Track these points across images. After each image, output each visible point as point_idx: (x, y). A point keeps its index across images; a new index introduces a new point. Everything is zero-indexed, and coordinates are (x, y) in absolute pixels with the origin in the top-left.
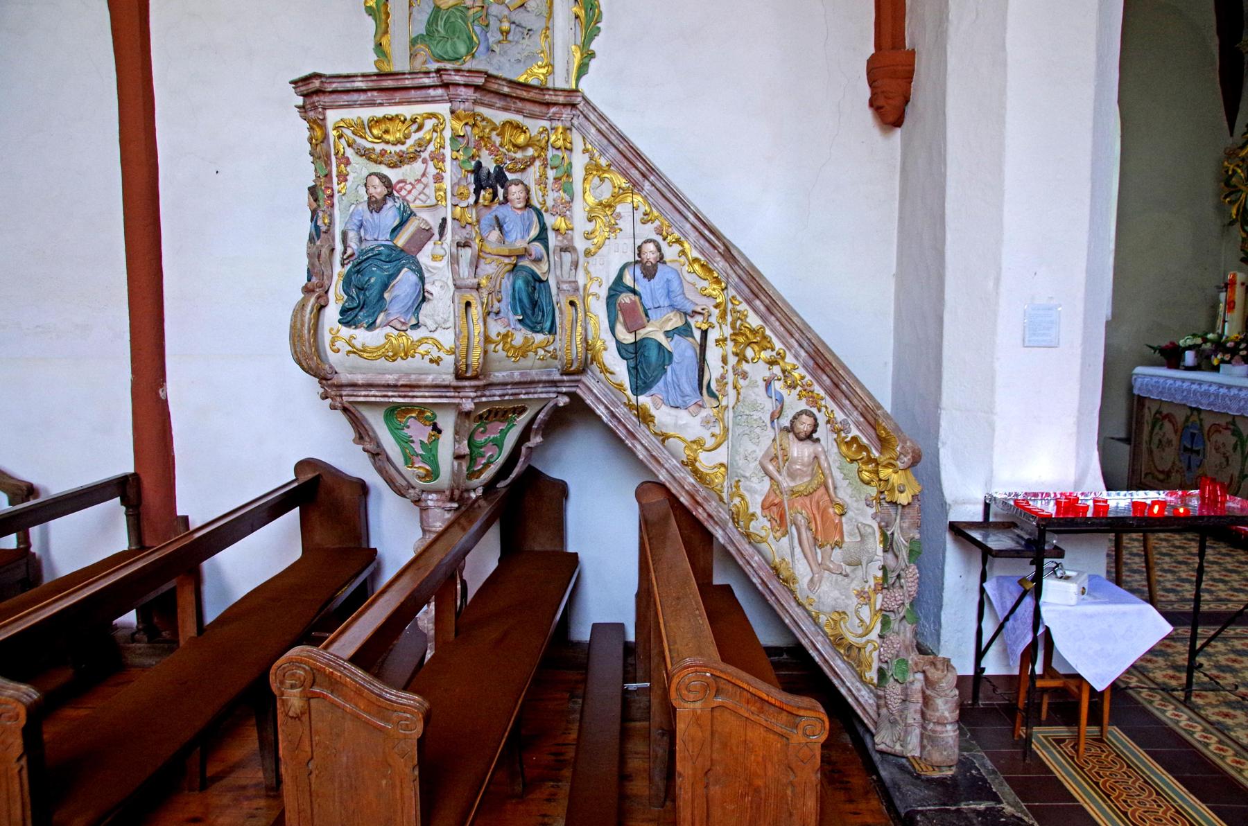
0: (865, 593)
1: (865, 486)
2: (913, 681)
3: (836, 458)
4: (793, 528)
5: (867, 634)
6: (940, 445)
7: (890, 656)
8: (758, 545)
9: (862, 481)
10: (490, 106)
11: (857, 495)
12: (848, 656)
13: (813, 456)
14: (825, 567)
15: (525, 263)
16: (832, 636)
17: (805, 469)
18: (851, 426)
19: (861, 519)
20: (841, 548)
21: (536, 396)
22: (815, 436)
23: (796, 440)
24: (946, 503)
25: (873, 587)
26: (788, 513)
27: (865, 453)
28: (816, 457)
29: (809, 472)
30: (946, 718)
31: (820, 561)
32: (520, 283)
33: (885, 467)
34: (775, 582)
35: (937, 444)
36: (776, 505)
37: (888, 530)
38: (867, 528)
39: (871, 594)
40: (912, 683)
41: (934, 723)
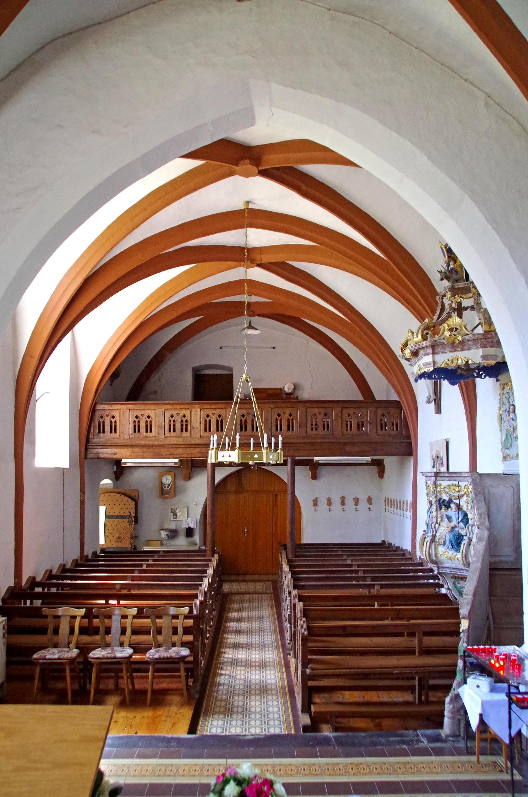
10: (444, 480)
15: (457, 529)
21: (464, 574)
32: (451, 536)
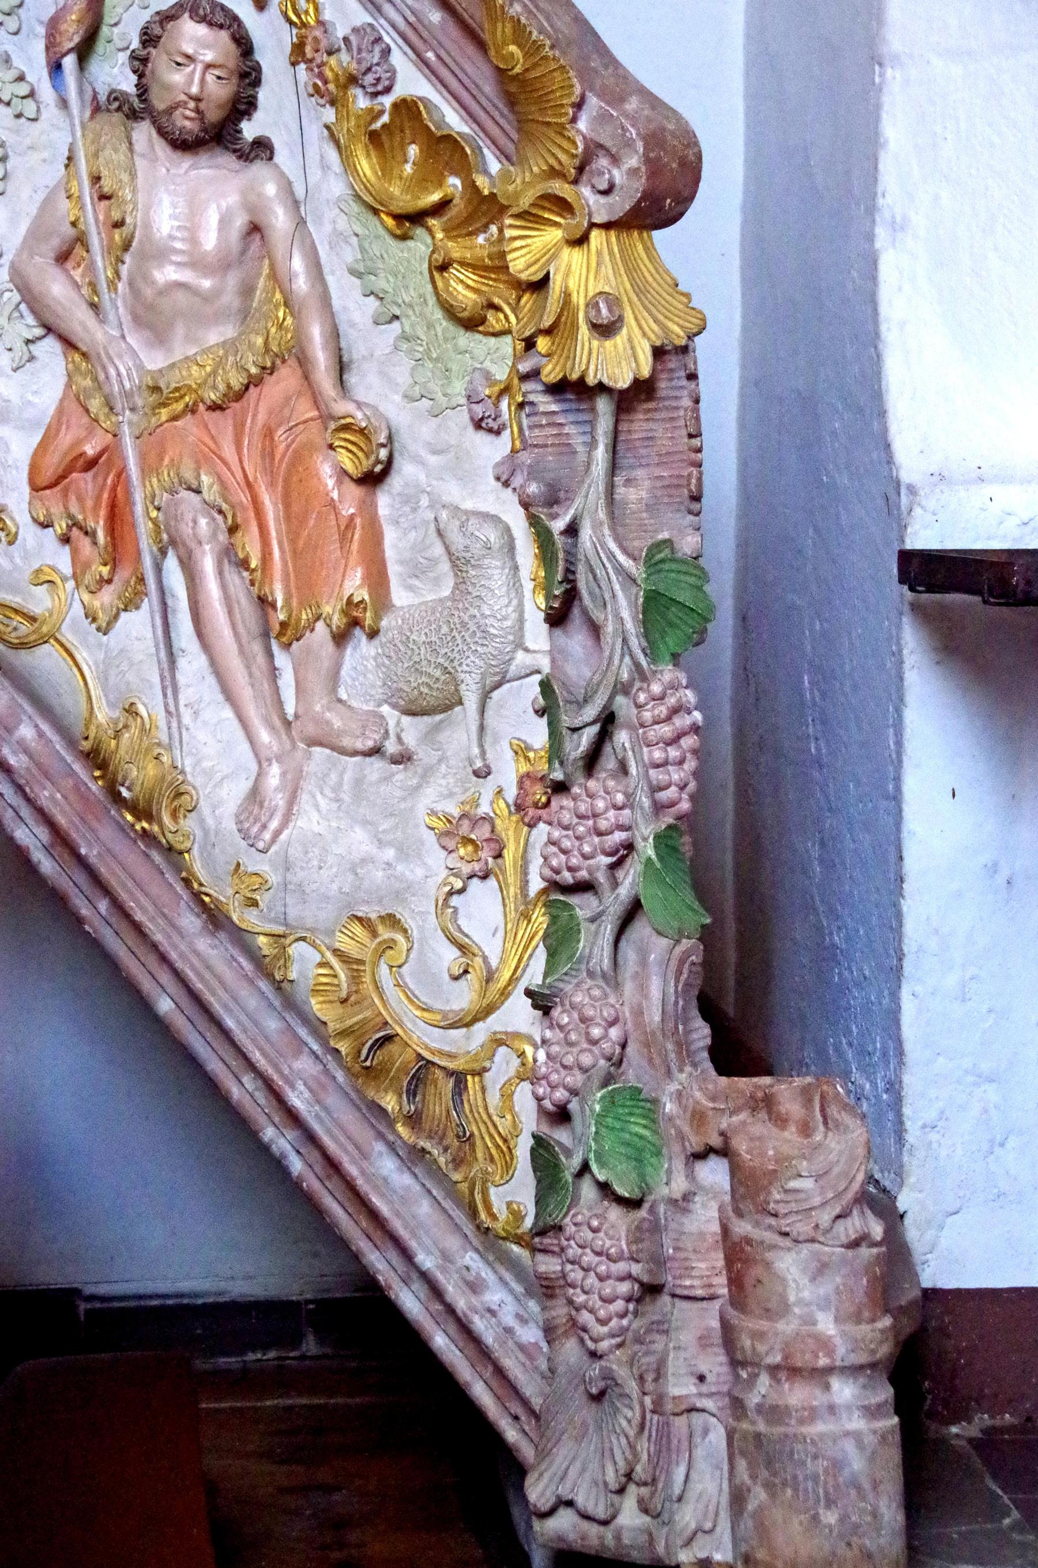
0: (476, 822)
1: (465, 339)
2: (687, 1197)
3: (342, 223)
4: (171, 563)
5: (487, 1011)
6: (881, 234)
7: (575, 1079)
8: (23, 659)
9: (450, 311)
11: (435, 387)
12: (414, 1120)
13: (240, 222)
14: (311, 730)
16: (343, 1034)
17: (206, 284)
18: (400, 60)
19: (453, 492)
20: (373, 634)
22: (249, 130)
23: (161, 148)
24: (898, 484)
25: (511, 792)
26: (138, 497)
27: (454, 183)
28: (255, 229)
29: (230, 298)
30: (824, 1344)
31: (290, 709)
33: (530, 218)
34: (107, 833)
35: (870, 238)
36: (91, 464)
37: (554, 517)
38: (473, 524)
39: (508, 828)
40: (682, 1204)
41: (774, 1370)
